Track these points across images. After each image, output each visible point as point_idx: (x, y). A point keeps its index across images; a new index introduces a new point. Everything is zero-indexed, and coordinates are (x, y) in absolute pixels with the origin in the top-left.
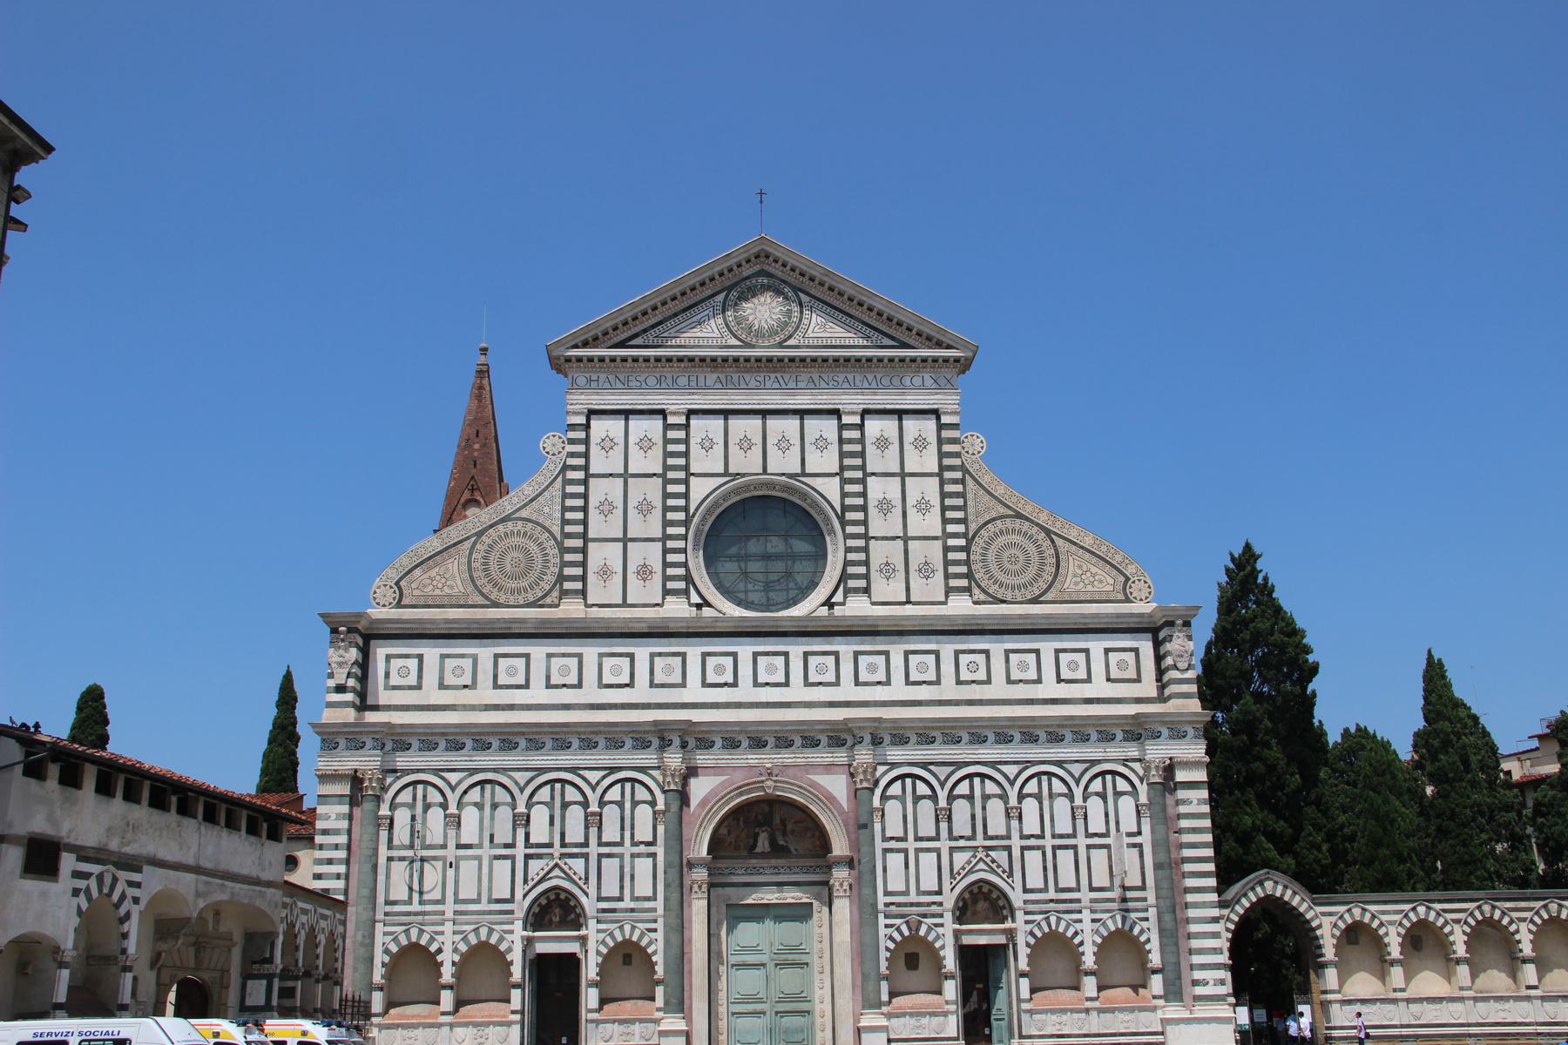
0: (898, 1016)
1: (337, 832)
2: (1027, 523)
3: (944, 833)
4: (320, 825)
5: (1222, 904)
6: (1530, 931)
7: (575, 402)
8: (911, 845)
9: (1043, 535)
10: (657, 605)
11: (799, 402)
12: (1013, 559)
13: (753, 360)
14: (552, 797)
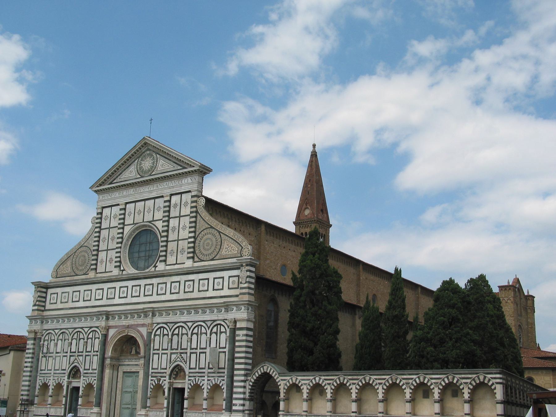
4: (27, 347)
6: (356, 388)
8: (161, 352)
9: (218, 234)
11: (153, 195)
12: (208, 244)
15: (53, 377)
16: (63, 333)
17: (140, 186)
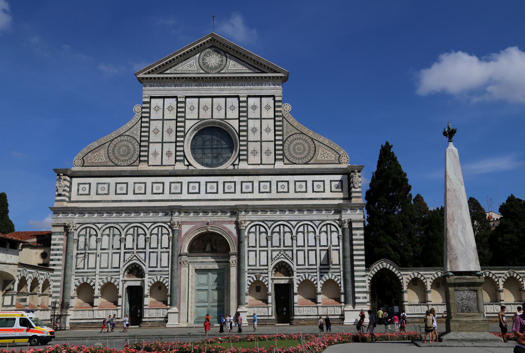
0: (251, 307)
1: (58, 245)
2: (305, 136)
3: (270, 245)
4: (52, 242)
5: (367, 271)
7: (145, 94)
8: (258, 249)
9: (310, 140)
10: (173, 165)
12: (299, 149)
13: (208, 78)
14: (134, 232)
15: (99, 276)
16: (110, 227)
17: (207, 82)
